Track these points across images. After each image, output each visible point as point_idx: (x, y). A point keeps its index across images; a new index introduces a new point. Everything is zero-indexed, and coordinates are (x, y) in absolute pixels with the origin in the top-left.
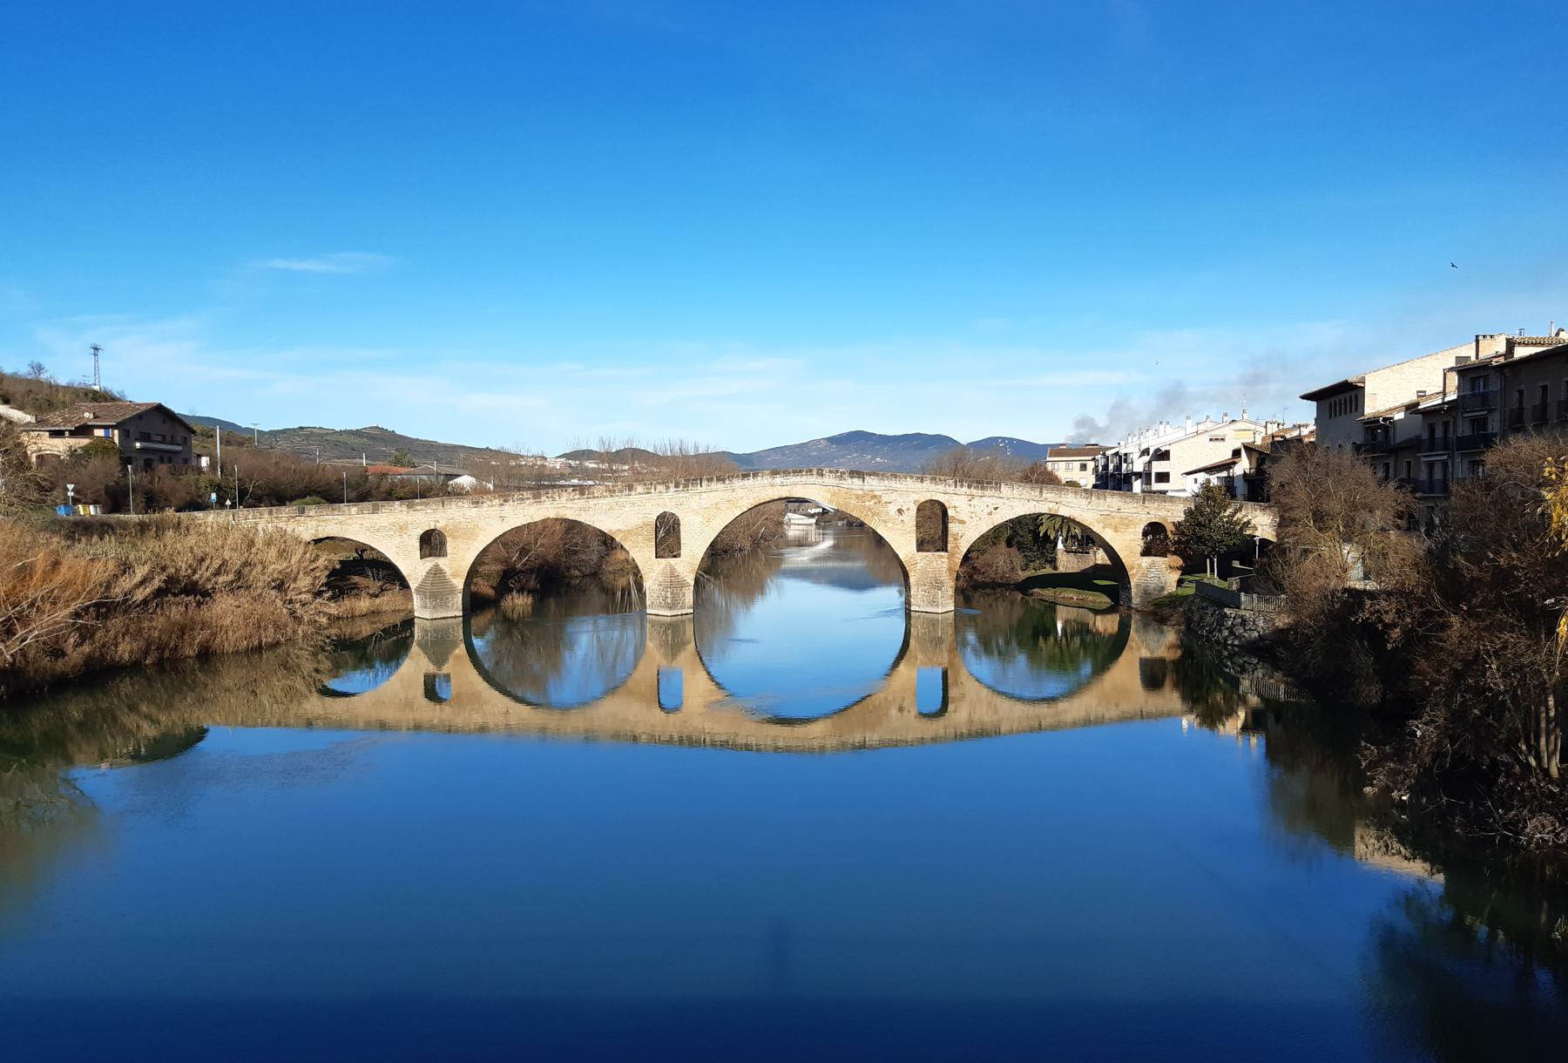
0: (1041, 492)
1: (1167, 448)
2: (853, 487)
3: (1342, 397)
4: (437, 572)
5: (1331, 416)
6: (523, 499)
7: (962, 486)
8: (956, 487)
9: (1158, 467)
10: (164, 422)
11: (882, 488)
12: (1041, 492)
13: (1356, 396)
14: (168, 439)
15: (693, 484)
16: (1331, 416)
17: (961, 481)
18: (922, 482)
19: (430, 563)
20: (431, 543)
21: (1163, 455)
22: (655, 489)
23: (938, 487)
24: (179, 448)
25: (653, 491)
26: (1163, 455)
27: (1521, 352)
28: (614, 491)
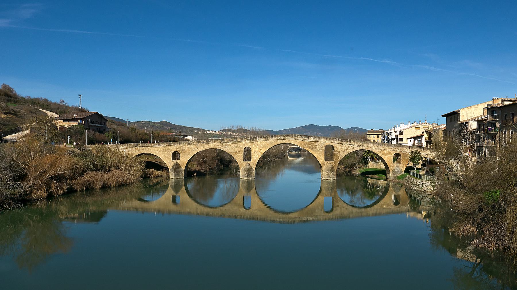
0: (363, 143)
1: (402, 131)
2: (305, 140)
3: (453, 116)
4: (177, 165)
8: (337, 141)
9: (400, 137)
10: (98, 118)
11: (314, 141)
14: (99, 123)
15: (255, 138)
17: (339, 139)
18: (326, 139)
19: (174, 162)
20: (175, 155)
22: (244, 140)
23: (332, 141)
24: (103, 126)
25: (243, 140)
26: (401, 133)
28: (231, 140)
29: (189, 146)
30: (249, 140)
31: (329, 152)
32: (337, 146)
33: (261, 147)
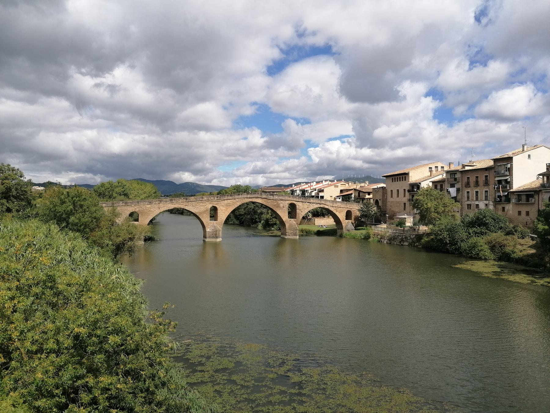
0: (321, 201)
1: (323, 189)
5: (393, 182)
6: (166, 201)
7: (300, 199)
9: (321, 194)
12: (321, 201)
13: (405, 177)
16: (393, 182)
21: (322, 191)
27: (467, 168)
29: (149, 206)
30: (216, 199)
31: (292, 210)
32: (299, 204)
33: (228, 205)
